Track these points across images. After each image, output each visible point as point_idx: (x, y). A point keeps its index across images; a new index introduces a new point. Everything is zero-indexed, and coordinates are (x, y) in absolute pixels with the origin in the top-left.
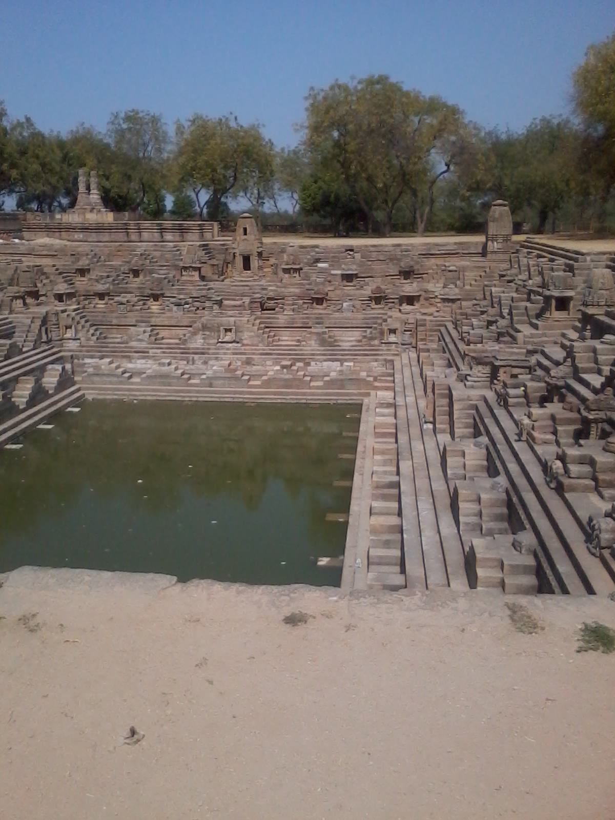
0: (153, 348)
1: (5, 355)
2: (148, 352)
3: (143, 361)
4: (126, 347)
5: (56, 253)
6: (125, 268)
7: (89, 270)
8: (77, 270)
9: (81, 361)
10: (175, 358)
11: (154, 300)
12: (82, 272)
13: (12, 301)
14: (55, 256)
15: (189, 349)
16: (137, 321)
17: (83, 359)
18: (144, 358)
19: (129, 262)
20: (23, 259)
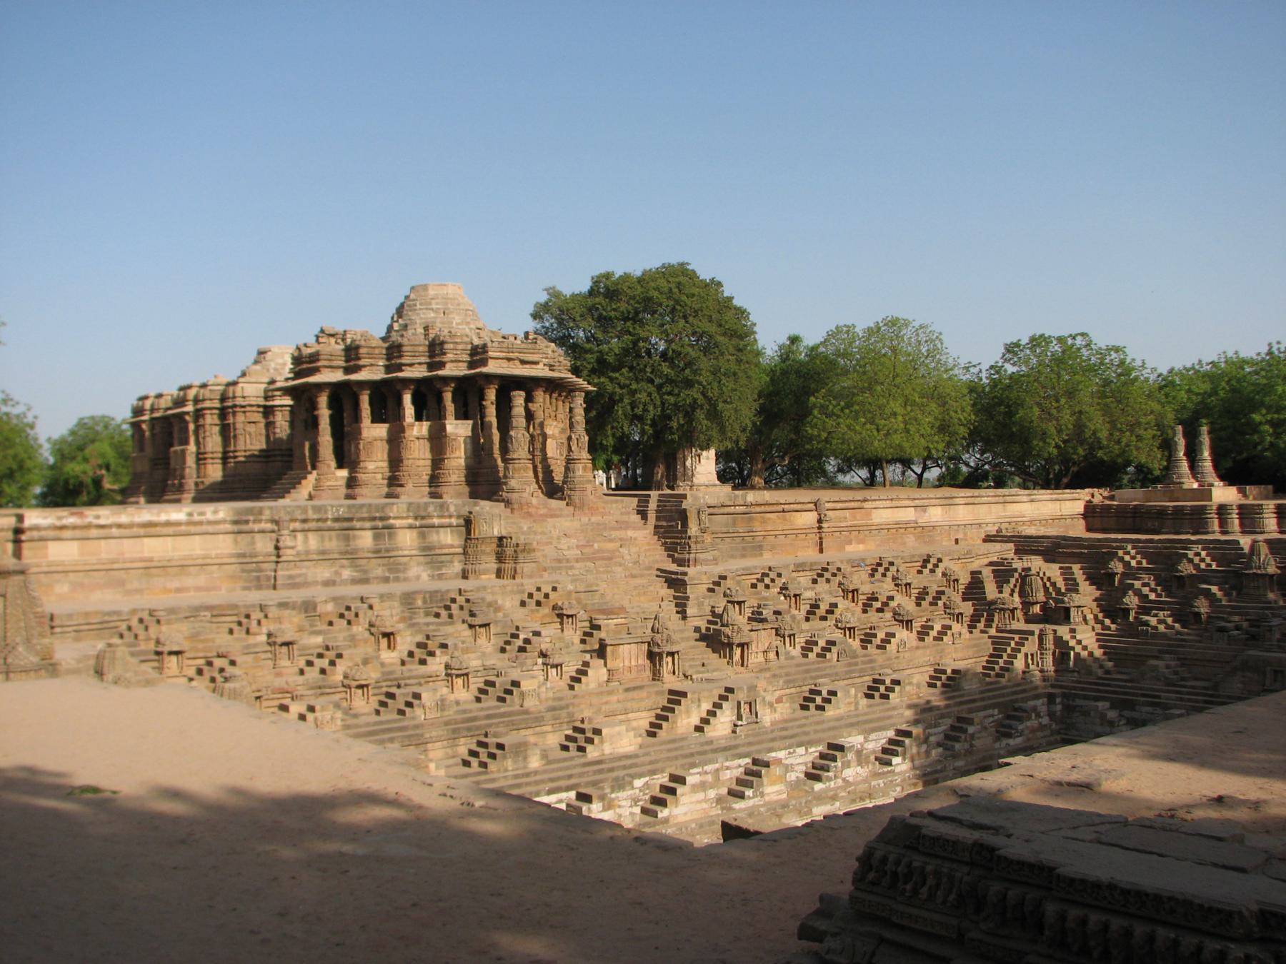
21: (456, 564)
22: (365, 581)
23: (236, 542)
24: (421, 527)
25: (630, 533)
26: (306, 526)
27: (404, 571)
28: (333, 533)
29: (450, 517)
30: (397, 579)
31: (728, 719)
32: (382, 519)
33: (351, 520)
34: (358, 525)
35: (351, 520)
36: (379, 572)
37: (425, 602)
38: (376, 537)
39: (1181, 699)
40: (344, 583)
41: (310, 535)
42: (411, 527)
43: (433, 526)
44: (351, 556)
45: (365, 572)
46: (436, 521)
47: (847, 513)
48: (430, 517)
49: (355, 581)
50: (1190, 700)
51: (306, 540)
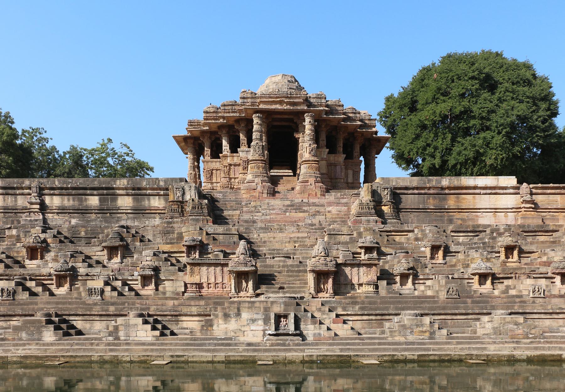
21: (157, 219)
23: (4, 200)
25: (330, 209)
26: (52, 192)
28: (71, 197)
29: (161, 189)
31: (262, 328)
32: (107, 189)
33: (85, 189)
34: (88, 192)
35: (85, 189)
41: (54, 197)
42: (127, 195)
43: (146, 195)
46: (148, 192)
47: (558, 197)
48: (146, 189)
51: (52, 199)
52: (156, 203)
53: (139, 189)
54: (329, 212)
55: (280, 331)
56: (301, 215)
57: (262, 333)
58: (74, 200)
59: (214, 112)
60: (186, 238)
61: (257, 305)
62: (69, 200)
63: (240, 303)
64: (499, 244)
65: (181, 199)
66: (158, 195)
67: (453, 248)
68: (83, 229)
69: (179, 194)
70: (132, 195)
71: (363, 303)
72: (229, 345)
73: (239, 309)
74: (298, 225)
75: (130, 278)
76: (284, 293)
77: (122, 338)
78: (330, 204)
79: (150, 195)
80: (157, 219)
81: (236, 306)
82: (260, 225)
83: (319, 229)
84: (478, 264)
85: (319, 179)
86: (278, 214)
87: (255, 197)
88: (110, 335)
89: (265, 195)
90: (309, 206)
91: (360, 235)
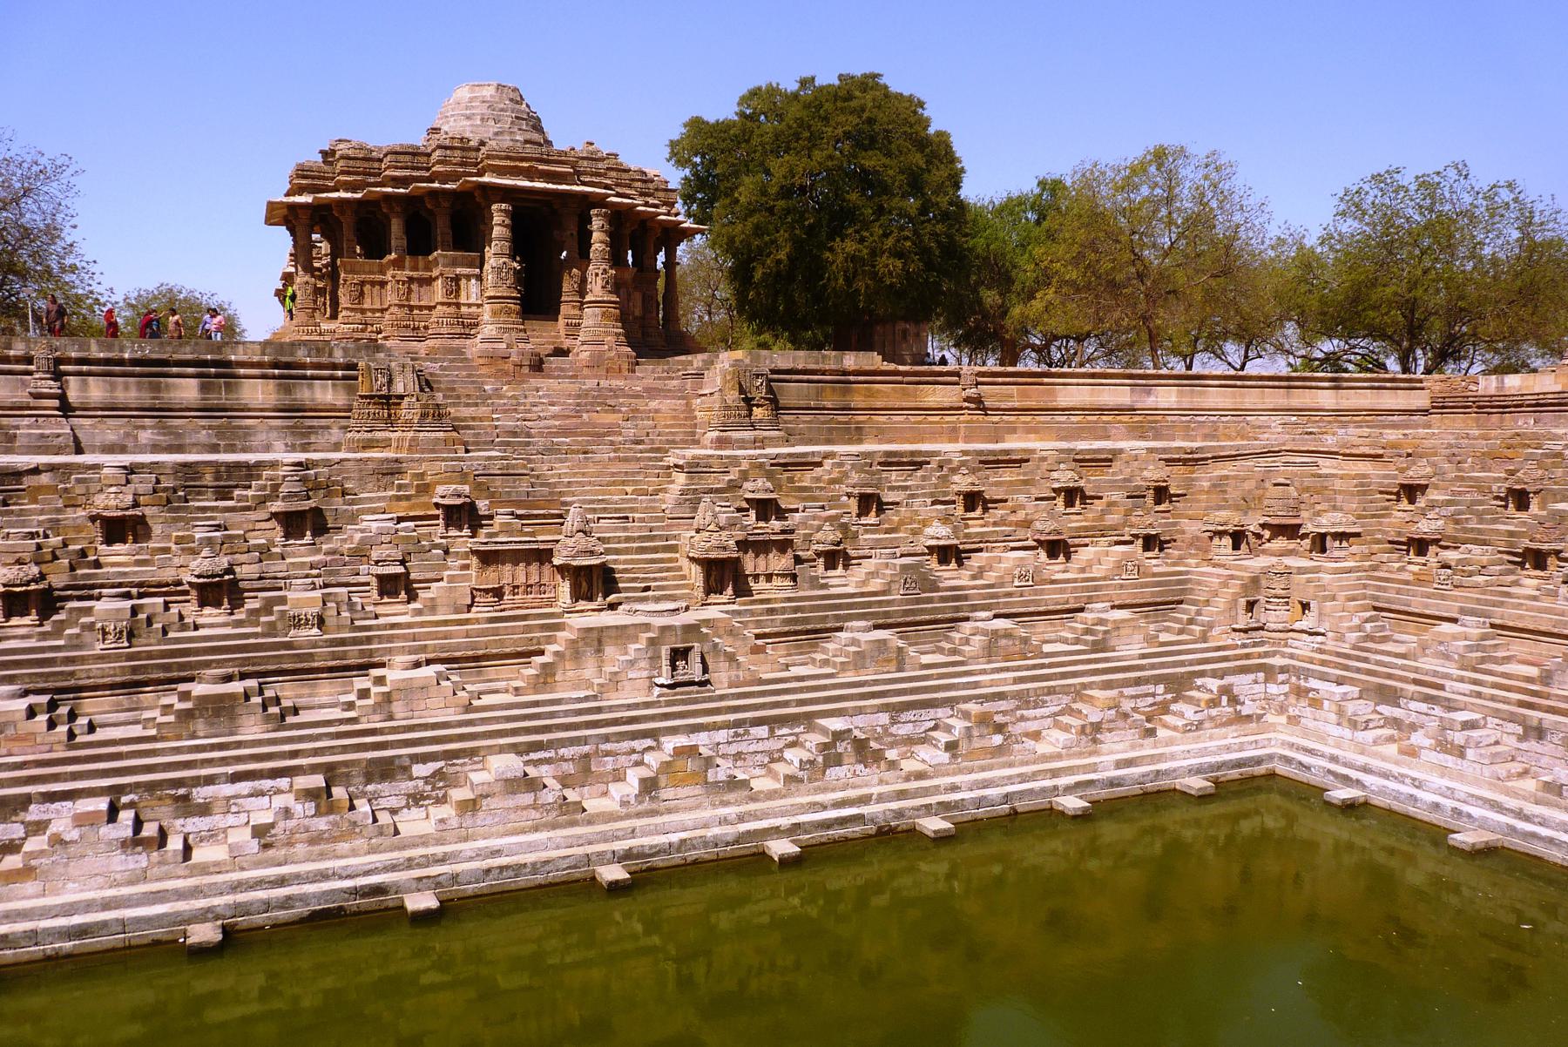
0: (1461, 680)
1: (1094, 643)
2: (1442, 687)
3: (1423, 707)
4: (1403, 668)
5: (1381, 452)
6: (1500, 488)
7: (1423, 488)
8: (1402, 486)
9: (1302, 683)
10: (1496, 713)
11: (1536, 567)
12: (1411, 491)
13: (1211, 538)
14: (1381, 456)
15: (1548, 696)
16: (1463, 611)
17: (1306, 680)
18: (1427, 699)
19: (1512, 473)
20: (1320, 462)
22: (179, 449)
24: (281, 377)
25: (654, 404)
27: (246, 435)
29: (335, 367)
30: (231, 449)
31: (645, 674)
32: (215, 364)
36: (203, 436)
37: (217, 479)
38: (204, 388)
39: (1479, 695)
40: (141, 450)
42: (264, 377)
43: (304, 377)
44: (161, 412)
45: (179, 435)
49: (156, 448)
50: (1493, 698)
51: (85, 383)
52: (326, 394)
53: (288, 366)
54: (657, 411)
55: (680, 679)
56: (610, 418)
57: (647, 683)
58: (139, 387)
59: (363, 159)
60: (440, 489)
61: (631, 631)
62: (126, 388)
63: (602, 629)
64: (956, 488)
65: (384, 391)
66: (332, 378)
67: (888, 497)
68: (209, 470)
69: (382, 380)
70: (274, 377)
71: (784, 610)
72: (599, 710)
73: (600, 642)
74: (612, 443)
75: (352, 580)
76: (657, 600)
77: (398, 716)
78: (652, 392)
79: (313, 378)
80: (335, 431)
81: (595, 635)
82: (540, 442)
83: (652, 450)
84: (939, 533)
85: (622, 338)
86: (568, 417)
87: (506, 373)
88: (374, 712)
89: (526, 370)
90: (617, 397)
91: (745, 476)
